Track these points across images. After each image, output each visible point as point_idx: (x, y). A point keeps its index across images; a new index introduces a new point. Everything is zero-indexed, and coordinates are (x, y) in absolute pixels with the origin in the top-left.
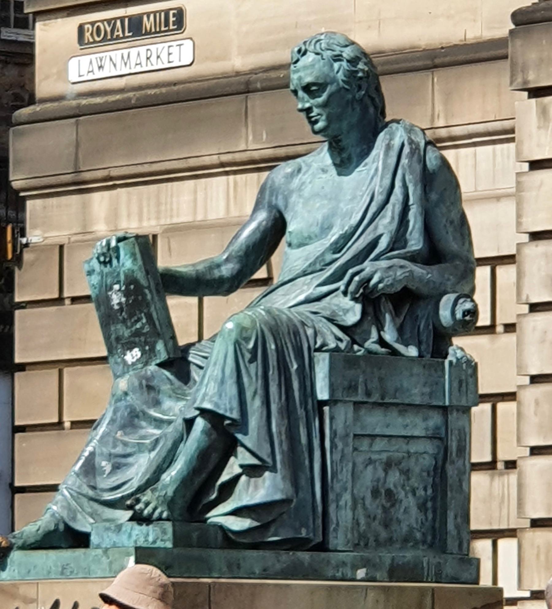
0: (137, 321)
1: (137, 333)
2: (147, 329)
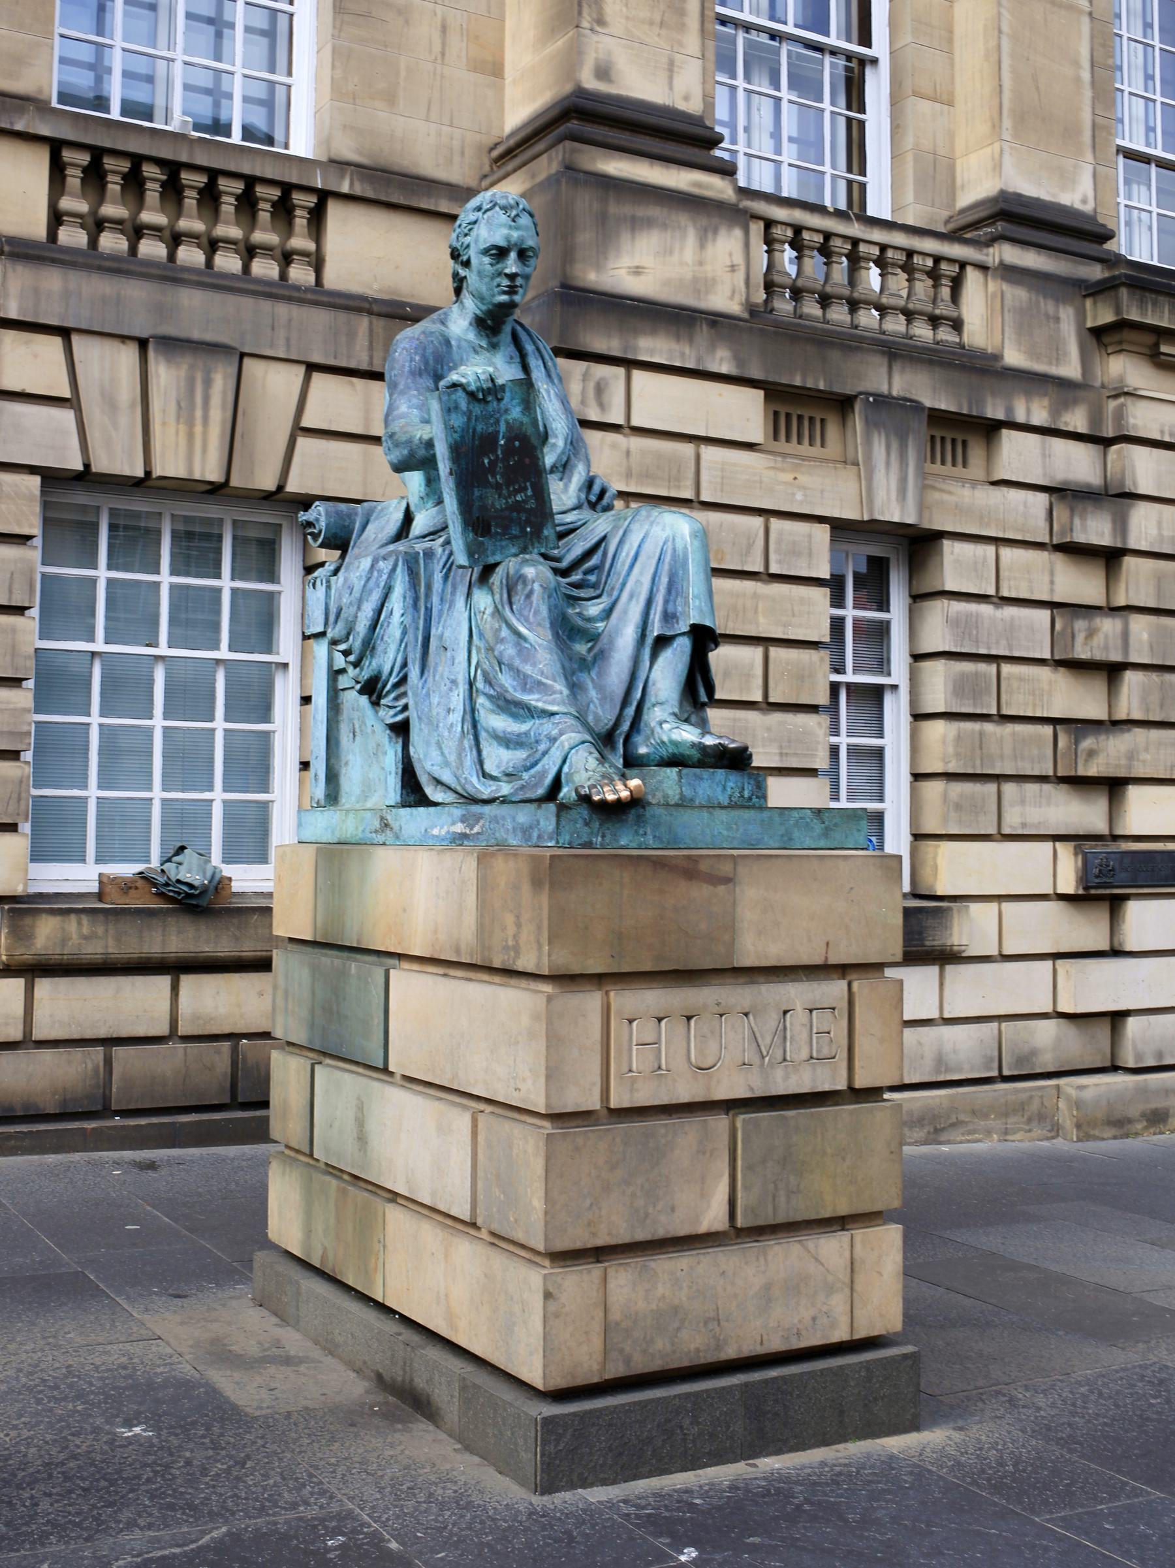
0: (516, 492)
1: (518, 507)
2: (532, 504)
